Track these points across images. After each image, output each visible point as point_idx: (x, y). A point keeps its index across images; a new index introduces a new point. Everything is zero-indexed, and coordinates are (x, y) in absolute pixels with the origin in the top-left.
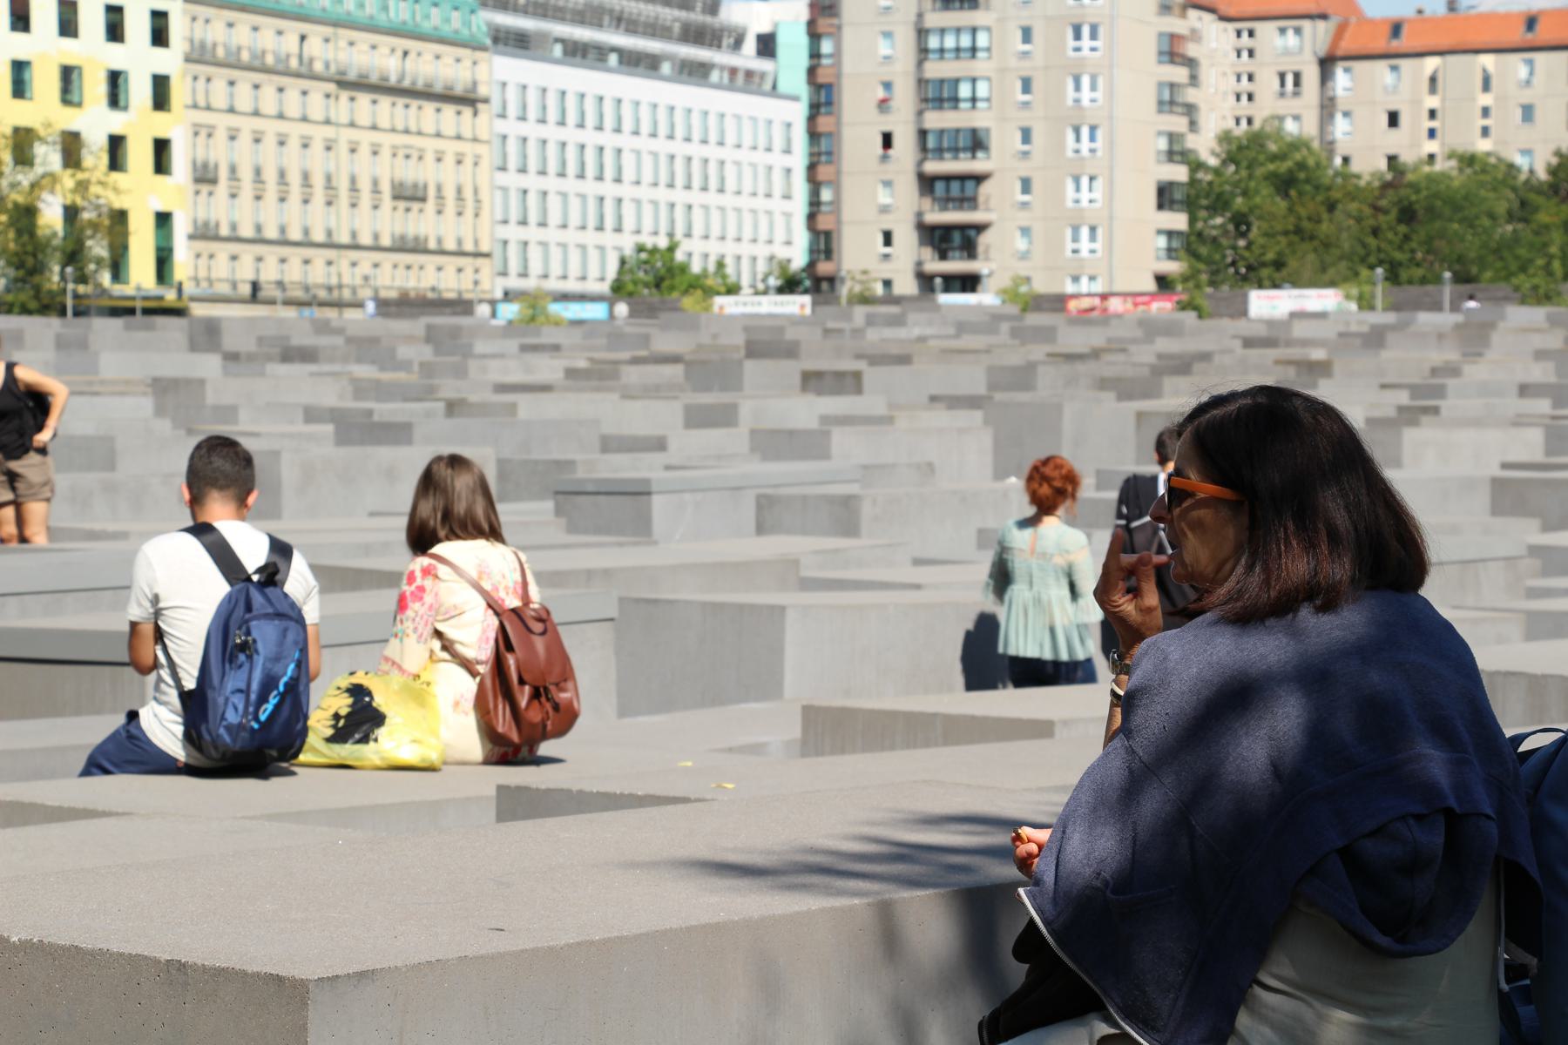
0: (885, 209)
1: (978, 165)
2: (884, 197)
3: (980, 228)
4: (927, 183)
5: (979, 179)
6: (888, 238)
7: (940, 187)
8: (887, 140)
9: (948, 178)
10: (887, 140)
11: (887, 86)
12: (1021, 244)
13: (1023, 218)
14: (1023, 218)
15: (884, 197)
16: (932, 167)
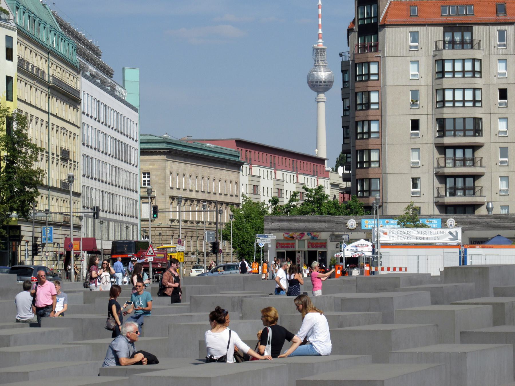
0: (414, 166)
1: (477, 140)
2: (414, 158)
3: (476, 177)
4: (442, 149)
5: (475, 148)
6: (415, 183)
7: (450, 153)
8: (415, 125)
9: (455, 147)
10: (415, 125)
11: (415, 93)
12: (503, 186)
13: (503, 171)
14: (503, 171)
15: (414, 158)
16: (447, 140)
